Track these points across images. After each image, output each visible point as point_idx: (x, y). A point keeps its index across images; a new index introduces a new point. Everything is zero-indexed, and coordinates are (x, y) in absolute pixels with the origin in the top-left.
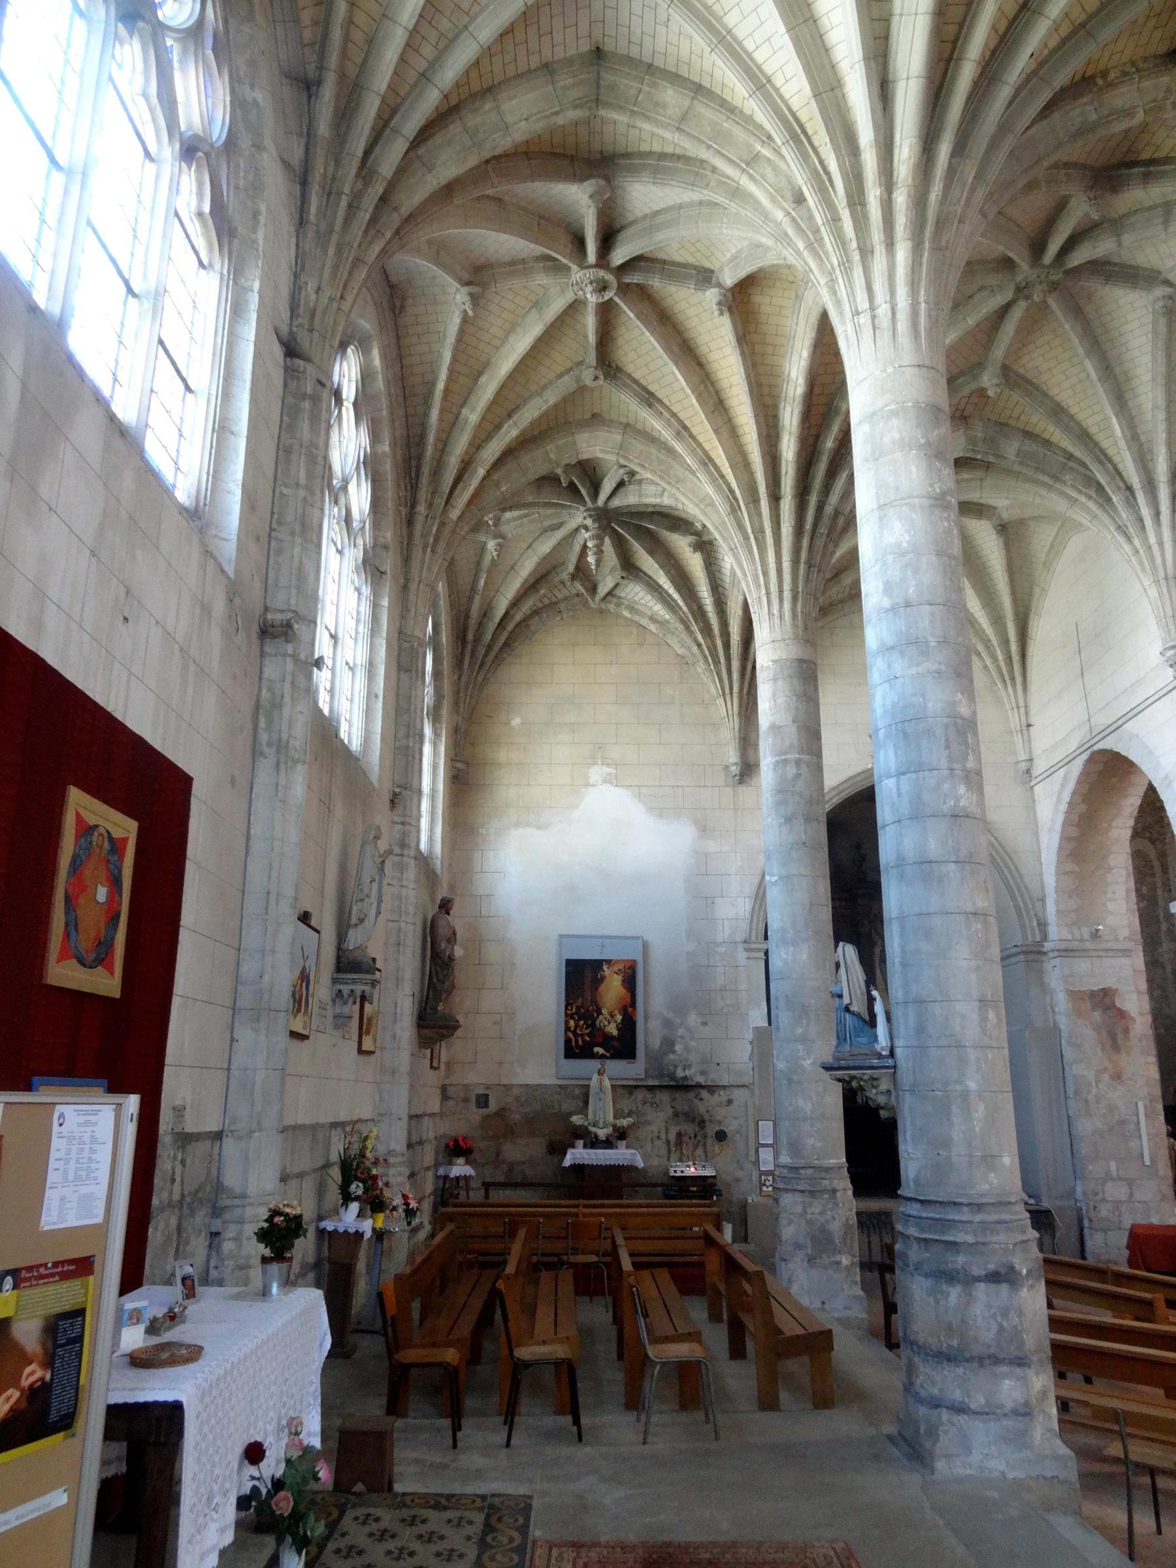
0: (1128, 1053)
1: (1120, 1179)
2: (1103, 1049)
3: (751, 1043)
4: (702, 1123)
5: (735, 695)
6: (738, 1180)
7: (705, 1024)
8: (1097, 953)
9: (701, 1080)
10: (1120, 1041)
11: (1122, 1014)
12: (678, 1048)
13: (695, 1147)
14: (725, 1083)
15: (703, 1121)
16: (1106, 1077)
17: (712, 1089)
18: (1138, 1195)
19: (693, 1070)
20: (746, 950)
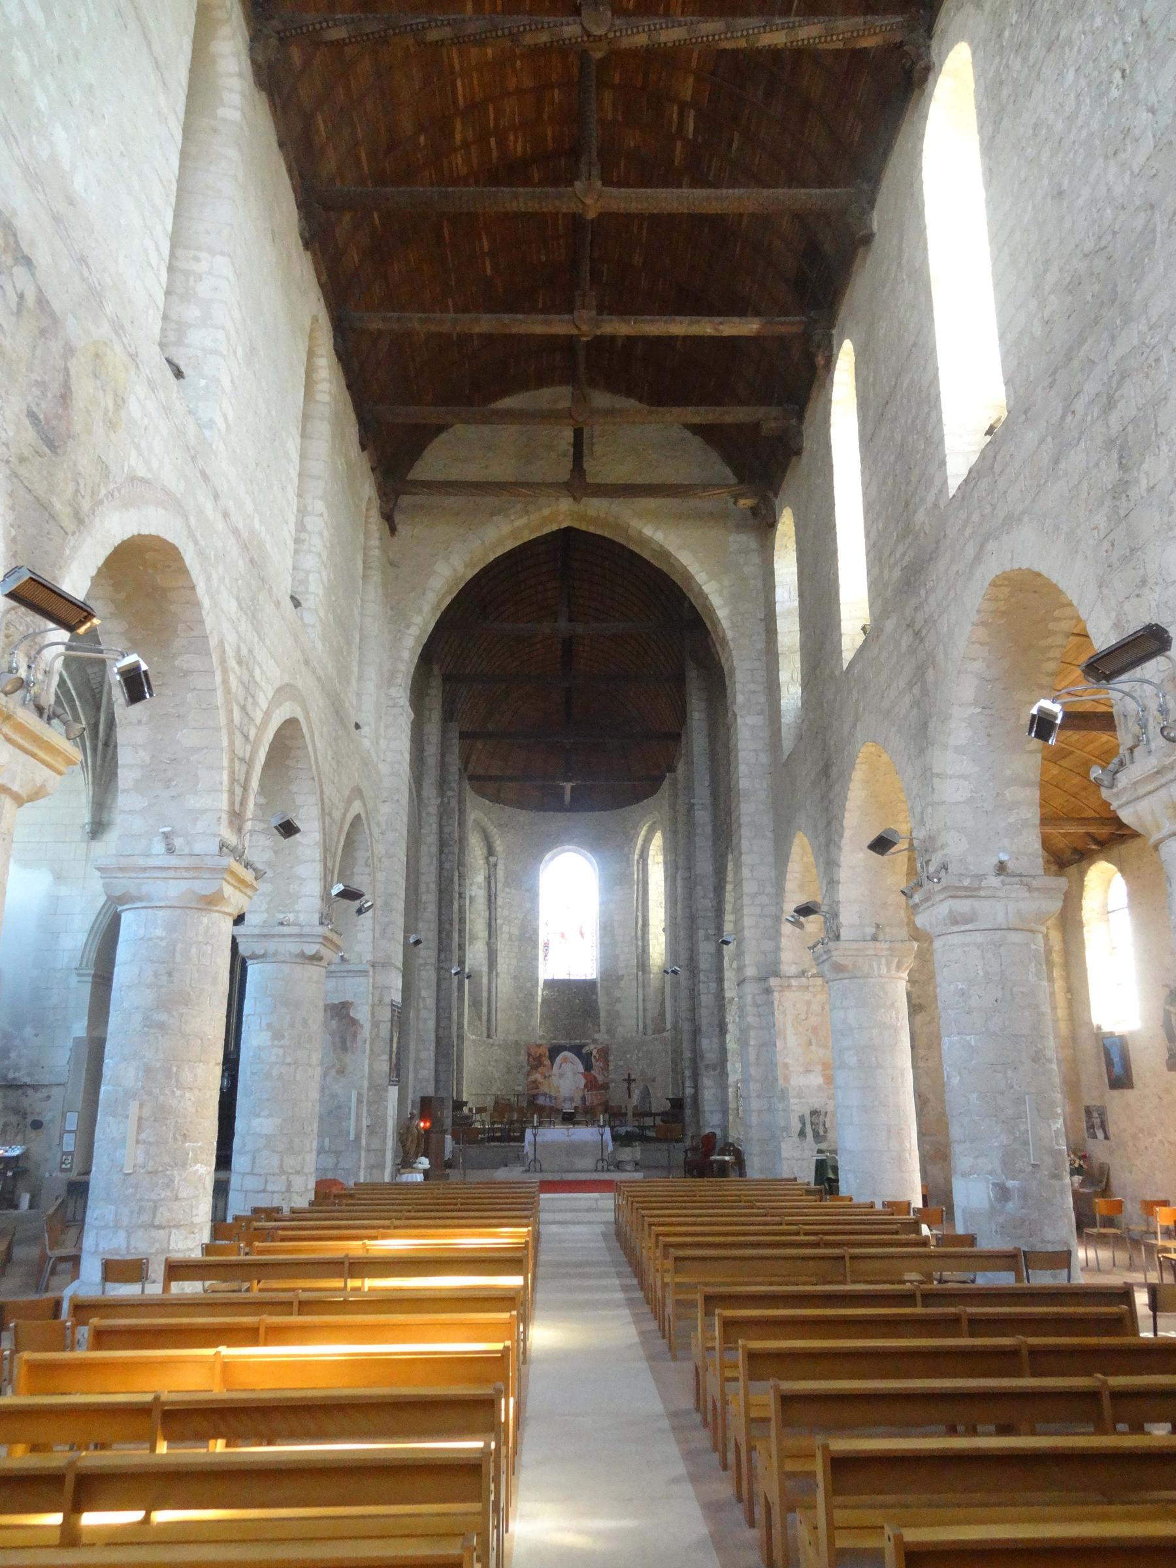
0: (353, 1053)
1: (330, 1151)
2: (334, 1050)
3: (71, 1050)
4: (24, 1117)
5: (90, 768)
6: (47, 1160)
7: (36, 1035)
8: (339, 974)
9: (28, 1080)
10: (348, 1044)
11: (354, 1022)
12: (13, 1055)
13: (16, 1135)
14: (46, 1083)
15: (26, 1114)
16: (333, 1072)
17: (36, 1087)
18: (340, 1166)
19: (22, 1073)
20: (79, 975)
